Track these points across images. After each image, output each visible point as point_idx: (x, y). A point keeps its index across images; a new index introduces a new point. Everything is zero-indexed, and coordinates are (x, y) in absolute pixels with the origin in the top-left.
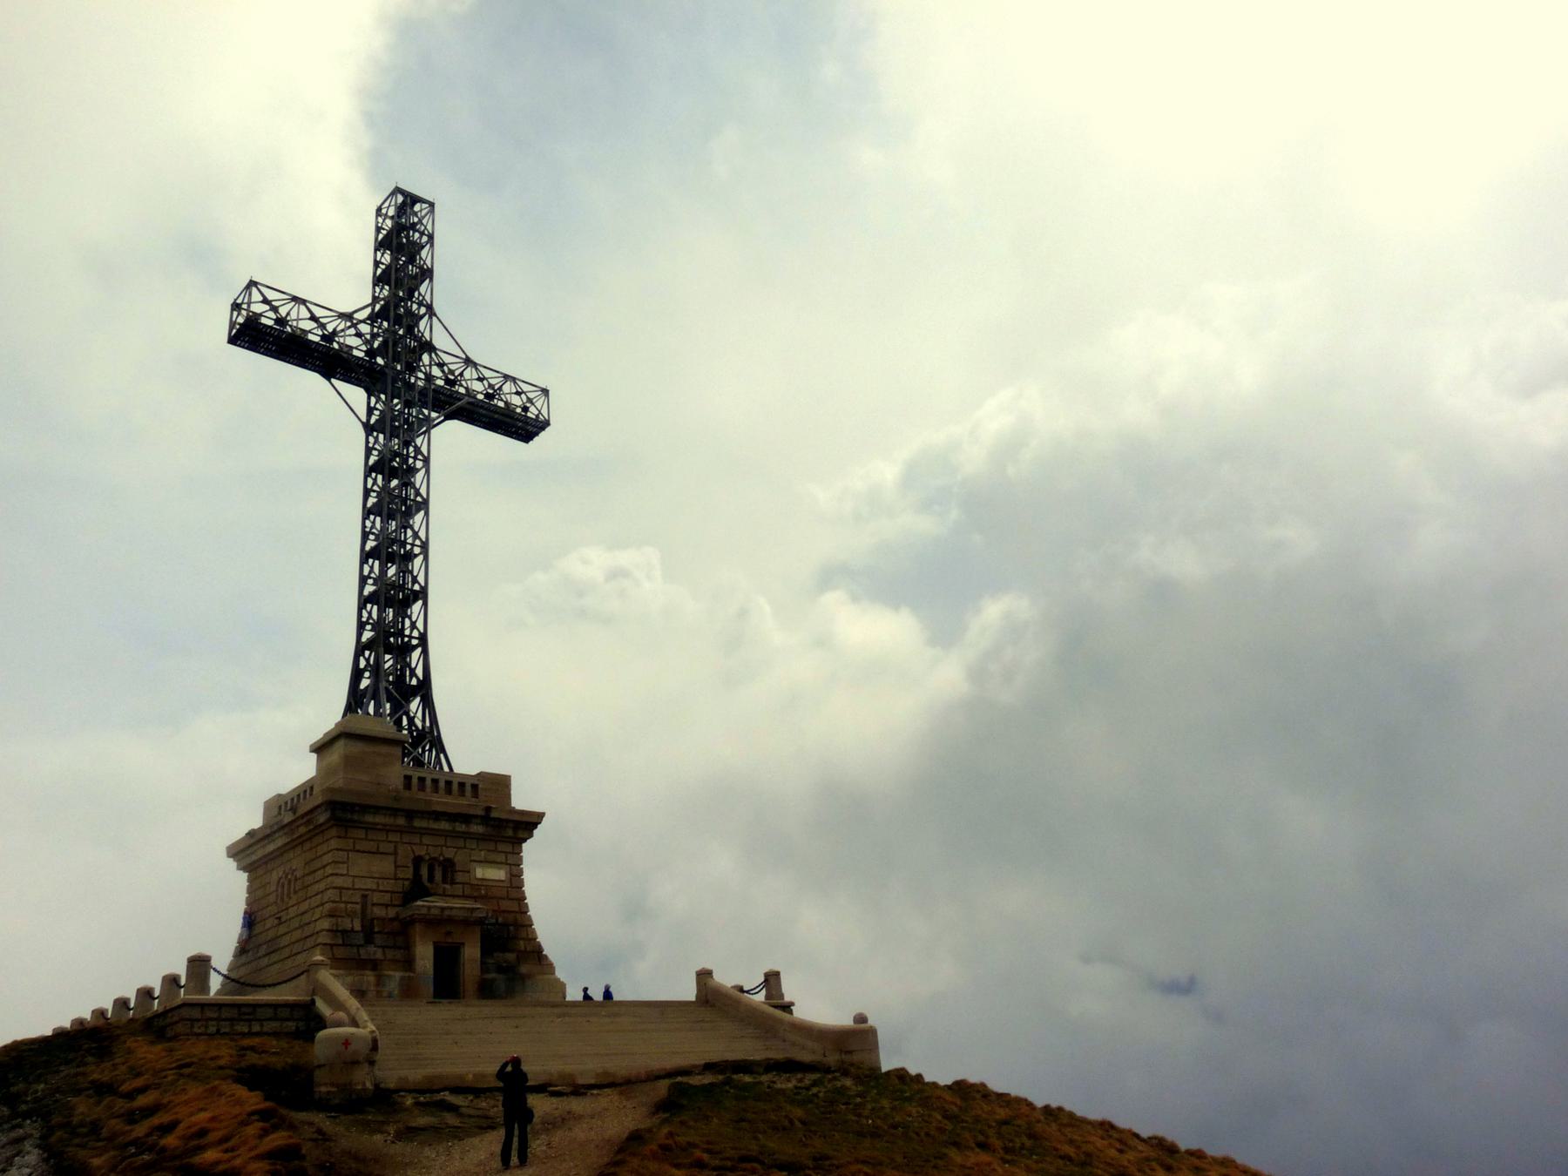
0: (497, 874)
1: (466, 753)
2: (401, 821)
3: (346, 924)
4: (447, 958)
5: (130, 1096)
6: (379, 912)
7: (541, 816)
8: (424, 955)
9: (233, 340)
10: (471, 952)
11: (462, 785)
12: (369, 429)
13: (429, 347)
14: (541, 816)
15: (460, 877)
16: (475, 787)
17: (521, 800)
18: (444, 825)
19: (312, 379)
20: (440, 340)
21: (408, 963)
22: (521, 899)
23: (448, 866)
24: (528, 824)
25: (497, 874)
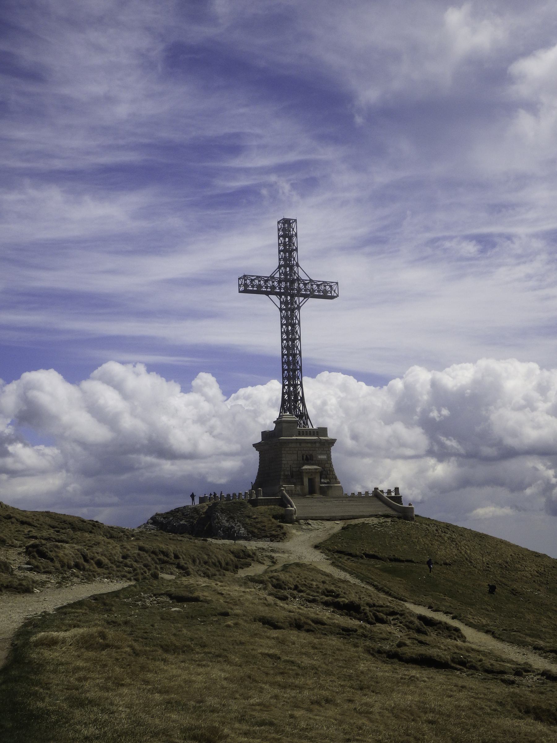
0: (324, 457)
1: (315, 422)
2: (298, 445)
3: (287, 473)
4: (311, 481)
5: (255, 519)
6: (294, 470)
7: (335, 440)
8: (306, 481)
9: (240, 292)
10: (317, 479)
11: (314, 432)
12: (281, 310)
13: (299, 279)
14: (335, 440)
15: (314, 459)
16: (317, 432)
17: (331, 435)
18: (309, 445)
19: (264, 296)
20: (303, 276)
21: (302, 484)
22: (331, 464)
23: (311, 456)
24: (332, 442)
25: (324, 457)
